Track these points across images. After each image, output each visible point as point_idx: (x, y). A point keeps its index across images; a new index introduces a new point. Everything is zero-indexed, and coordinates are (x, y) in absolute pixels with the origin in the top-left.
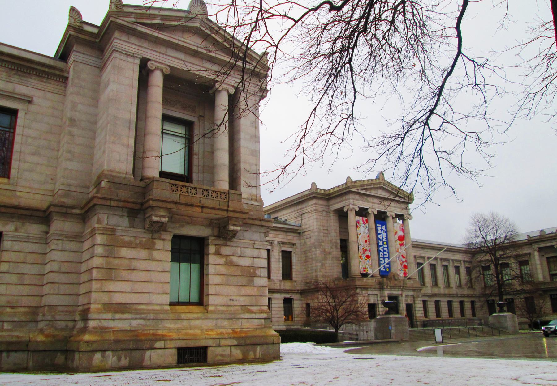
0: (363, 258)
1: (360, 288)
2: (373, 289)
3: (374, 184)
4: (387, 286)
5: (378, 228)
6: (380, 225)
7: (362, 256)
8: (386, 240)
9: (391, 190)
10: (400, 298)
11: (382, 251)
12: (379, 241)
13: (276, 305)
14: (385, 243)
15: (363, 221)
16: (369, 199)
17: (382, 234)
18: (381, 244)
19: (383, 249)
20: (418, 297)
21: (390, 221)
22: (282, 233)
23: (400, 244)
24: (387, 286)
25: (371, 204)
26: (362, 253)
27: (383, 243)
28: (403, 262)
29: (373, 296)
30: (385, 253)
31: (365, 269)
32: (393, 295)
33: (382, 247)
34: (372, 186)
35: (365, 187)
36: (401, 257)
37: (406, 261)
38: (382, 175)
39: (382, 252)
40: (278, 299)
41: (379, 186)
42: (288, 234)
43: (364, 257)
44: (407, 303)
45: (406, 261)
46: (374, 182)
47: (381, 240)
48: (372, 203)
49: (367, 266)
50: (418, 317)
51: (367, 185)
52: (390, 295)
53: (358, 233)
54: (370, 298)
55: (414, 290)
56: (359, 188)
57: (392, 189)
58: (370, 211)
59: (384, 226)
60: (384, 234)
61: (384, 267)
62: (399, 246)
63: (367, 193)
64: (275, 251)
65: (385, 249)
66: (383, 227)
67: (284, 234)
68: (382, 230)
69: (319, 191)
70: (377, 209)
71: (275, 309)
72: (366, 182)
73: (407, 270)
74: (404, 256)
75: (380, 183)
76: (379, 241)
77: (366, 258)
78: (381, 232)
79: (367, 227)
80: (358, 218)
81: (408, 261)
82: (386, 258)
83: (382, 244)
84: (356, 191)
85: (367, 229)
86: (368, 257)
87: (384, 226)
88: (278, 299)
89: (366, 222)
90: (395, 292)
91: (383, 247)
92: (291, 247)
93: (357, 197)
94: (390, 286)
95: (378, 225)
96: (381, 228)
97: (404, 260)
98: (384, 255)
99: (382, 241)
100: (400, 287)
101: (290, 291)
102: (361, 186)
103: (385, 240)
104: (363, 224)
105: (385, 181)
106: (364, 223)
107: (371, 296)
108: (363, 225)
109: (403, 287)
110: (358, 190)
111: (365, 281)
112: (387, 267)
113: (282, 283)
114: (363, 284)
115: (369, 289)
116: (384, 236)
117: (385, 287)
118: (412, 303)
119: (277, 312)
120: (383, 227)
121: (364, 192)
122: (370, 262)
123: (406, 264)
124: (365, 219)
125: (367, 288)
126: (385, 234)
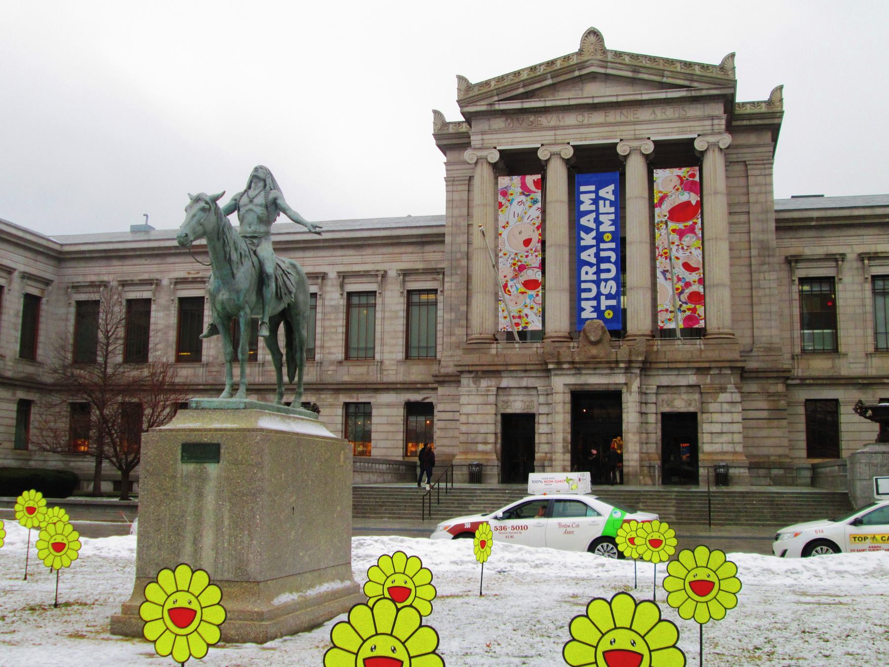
0: (513, 290)
1: (470, 372)
2: (523, 375)
3: (569, 69)
4: (559, 363)
5: (583, 197)
6: (592, 188)
7: (510, 284)
8: (613, 228)
9: (630, 74)
10: (625, 397)
11: (594, 261)
12: (583, 234)
13: (384, 420)
14: (607, 237)
15: (524, 186)
16: (544, 120)
17: (597, 211)
18: (588, 239)
19: (597, 255)
20: (723, 389)
21: (635, 170)
22: (410, 249)
23: (674, 231)
24: (559, 363)
25: (552, 133)
26: (511, 274)
27: (599, 238)
28: (688, 284)
29: (522, 392)
30: (603, 266)
31: (517, 321)
32: (586, 388)
33: (594, 250)
34: (549, 82)
35: (521, 90)
36: (680, 271)
37: (702, 281)
38: (592, 38)
39: (590, 265)
40: (389, 405)
41: (577, 73)
42: (428, 248)
43: (516, 287)
44: (667, 409)
45: (702, 281)
46: (574, 61)
47: (588, 230)
48: (555, 128)
49: (526, 311)
50: (710, 453)
51: (525, 83)
52: (578, 388)
53: (501, 224)
54: (511, 398)
55: (700, 371)
56: (496, 98)
57: (634, 71)
58: (542, 155)
59: (612, 187)
60: (606, 208)
61: (597, 309)
62: (675, 237)
63: (527, 105)
64: (388, 294)
65: (603, 254)
66: (608, 192)
67: (417, 249)
68: (595, 202)
69: (451, 130)
70: (571, 144)
71: (379, 428)
72: (524, 76)
73: (700, 309)
74: (694, 266)
75: (581, 66)
76: (583, 234)
77: (524, 290)
78: (593, 207)
79: (535, 202)
80: (504, 181)
81: (707, 283)
82: (606, 280)
83: (594, 242)
84: (484, 108)
85: (539, 205)
86: (530, 284)
87: (612, 187)
88: (389, 405)
89: (533, 188)
90: (596, 380)
91: (599, 250)
92: (435, 280)
93: (499, 123)
94: (573, 363)
95: (583, 189)
96: (593, 196)
97: (694, 277)
98: (598, 272)
99: (593, 234)
100: (617, 362)
101: (419, 386)
102: (499, 91)
103: (607, 227)
104: (523, 194)
105: (605, 51)
106: (525, 190)
107: (514, 392)
108: (523, 198)
109: (630, 362)
110: (491, 104)
111: (494, 351)
112: (608, 307)
113: (402, 369)
114: (486, 359)
115: (503, 375)
116: (602, 218)
117: (550, 366)
118: (692, 409)
119: (383, 436)
120: (608, 192)
121: (516, 105)
122: (539, 299)
123: (701, 290)
124: (530, 179)
125: (499, 372)
126: (612, 210)
